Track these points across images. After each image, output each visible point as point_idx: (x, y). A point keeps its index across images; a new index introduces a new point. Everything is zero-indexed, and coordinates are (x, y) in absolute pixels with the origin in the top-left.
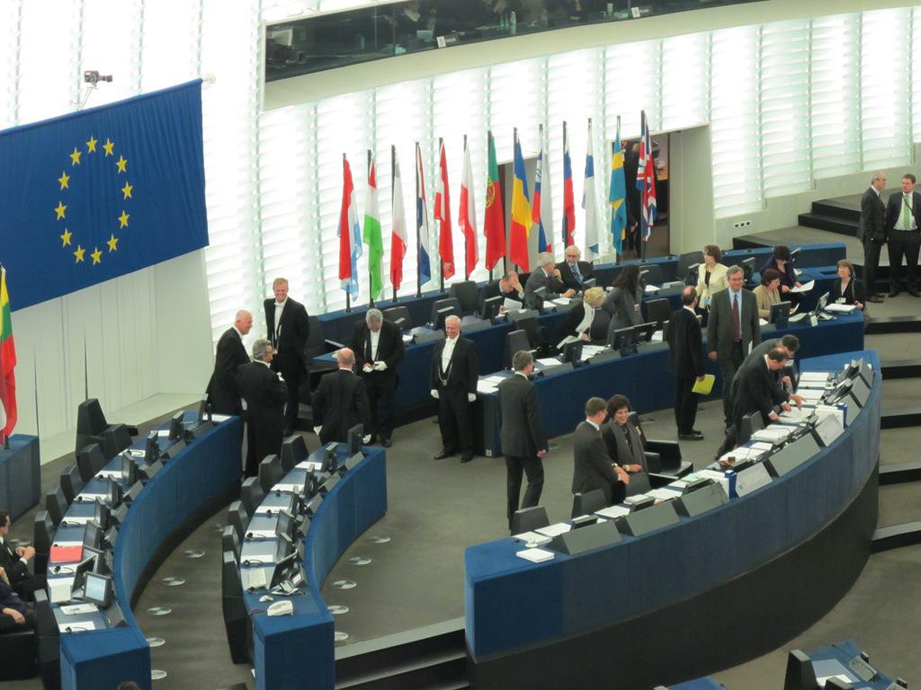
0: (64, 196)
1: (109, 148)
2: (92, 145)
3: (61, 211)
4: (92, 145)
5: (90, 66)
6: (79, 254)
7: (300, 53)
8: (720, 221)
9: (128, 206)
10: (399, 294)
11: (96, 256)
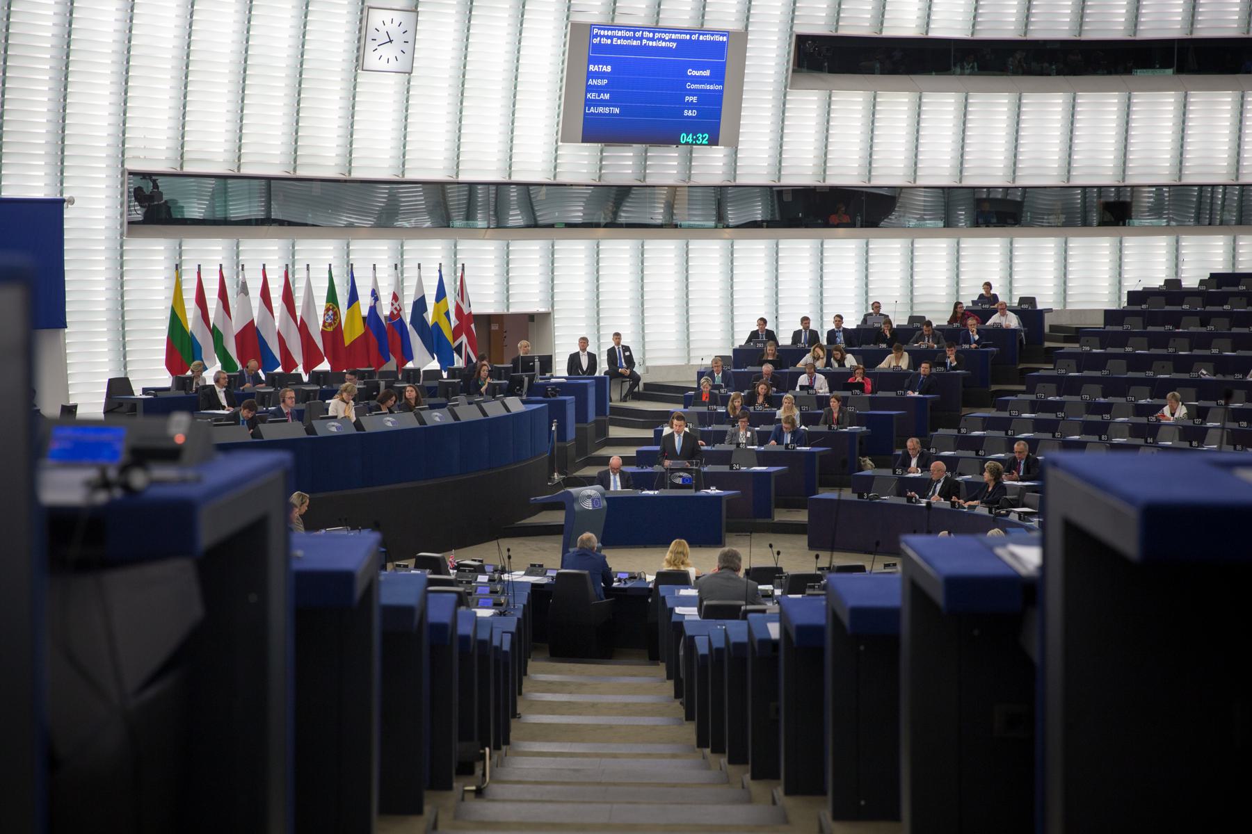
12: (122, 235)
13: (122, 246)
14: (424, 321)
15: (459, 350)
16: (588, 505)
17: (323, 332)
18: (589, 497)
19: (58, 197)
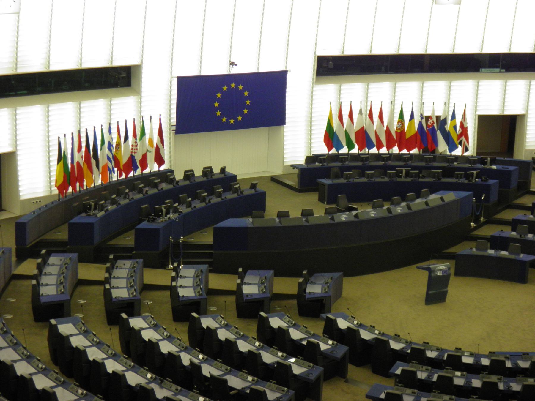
0: (218, 100)
1: (241, 87)
2: (233, 85)
3: (216, 104)
4: (233, 85)
5: (232, 61)
6: (224, 119)
7: (331, 67)
8: (527, 151)
9: (247, 107)
10: (350, 152)
11: (232, 121)
12: (313, 83)
13: (313, 88)
14: (445, 129)
15: (460, 143)
16: (440, 274)
17: (396, 132)
18: (441, 270)
19: (284, 69)
